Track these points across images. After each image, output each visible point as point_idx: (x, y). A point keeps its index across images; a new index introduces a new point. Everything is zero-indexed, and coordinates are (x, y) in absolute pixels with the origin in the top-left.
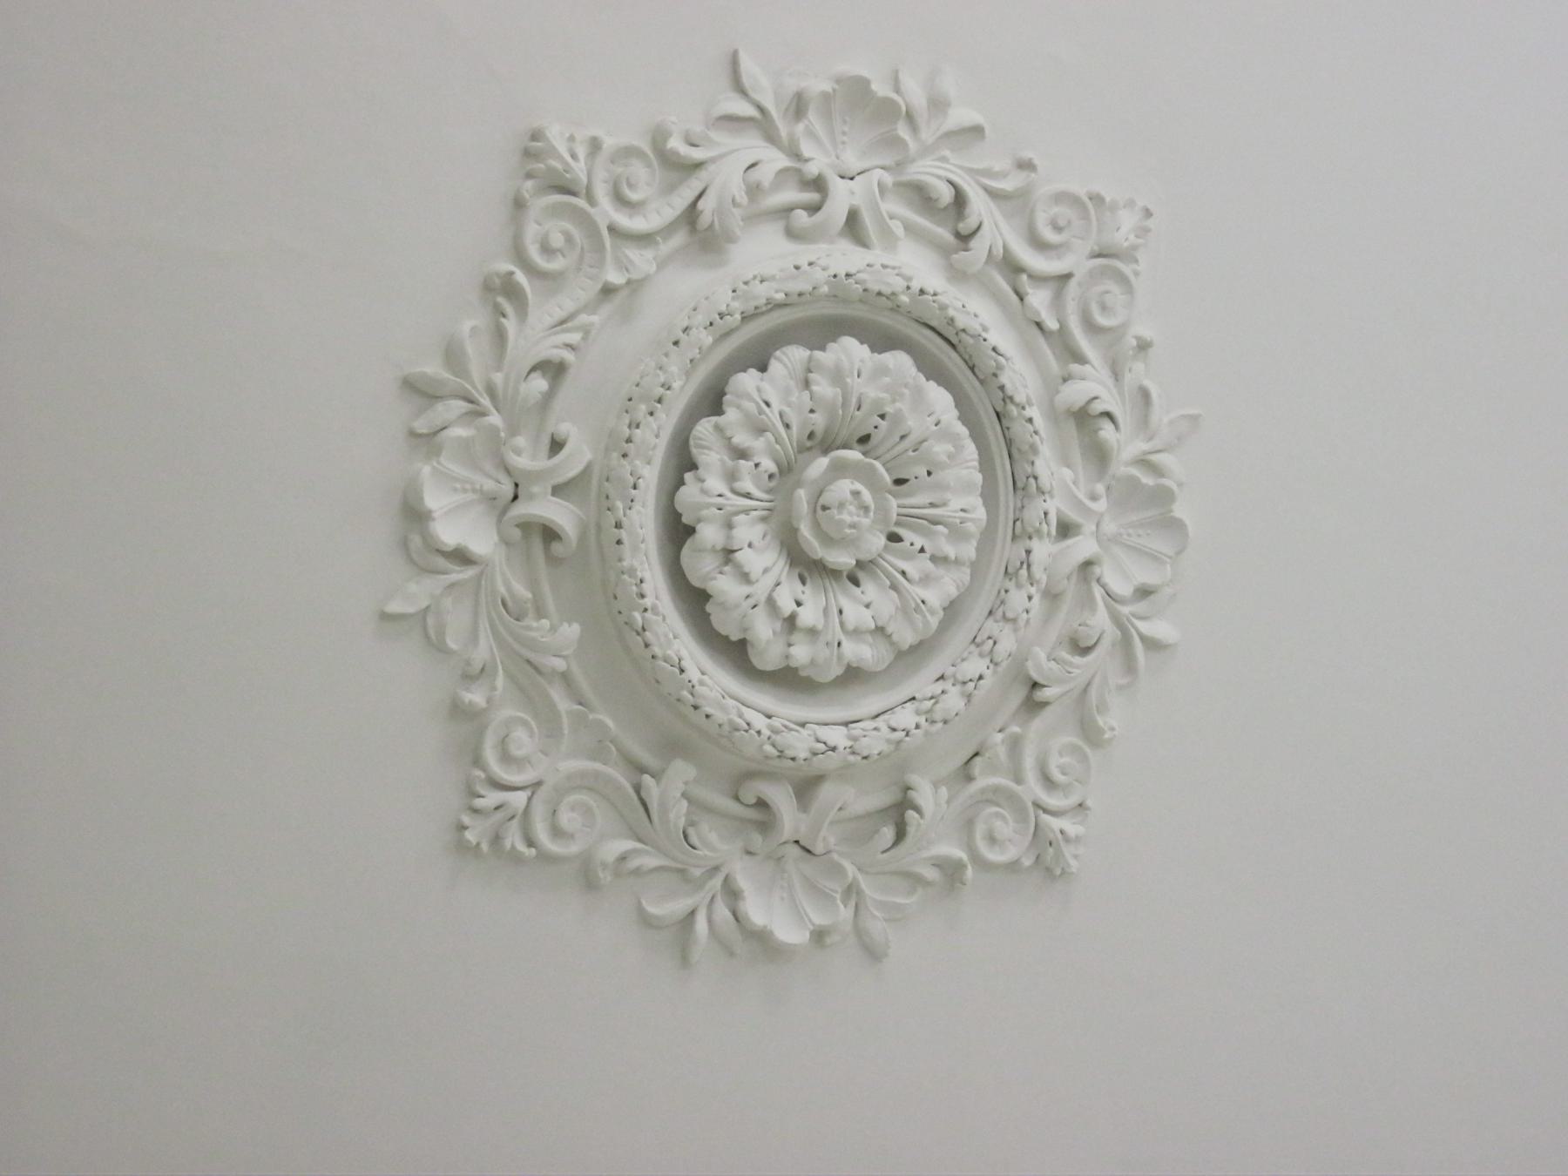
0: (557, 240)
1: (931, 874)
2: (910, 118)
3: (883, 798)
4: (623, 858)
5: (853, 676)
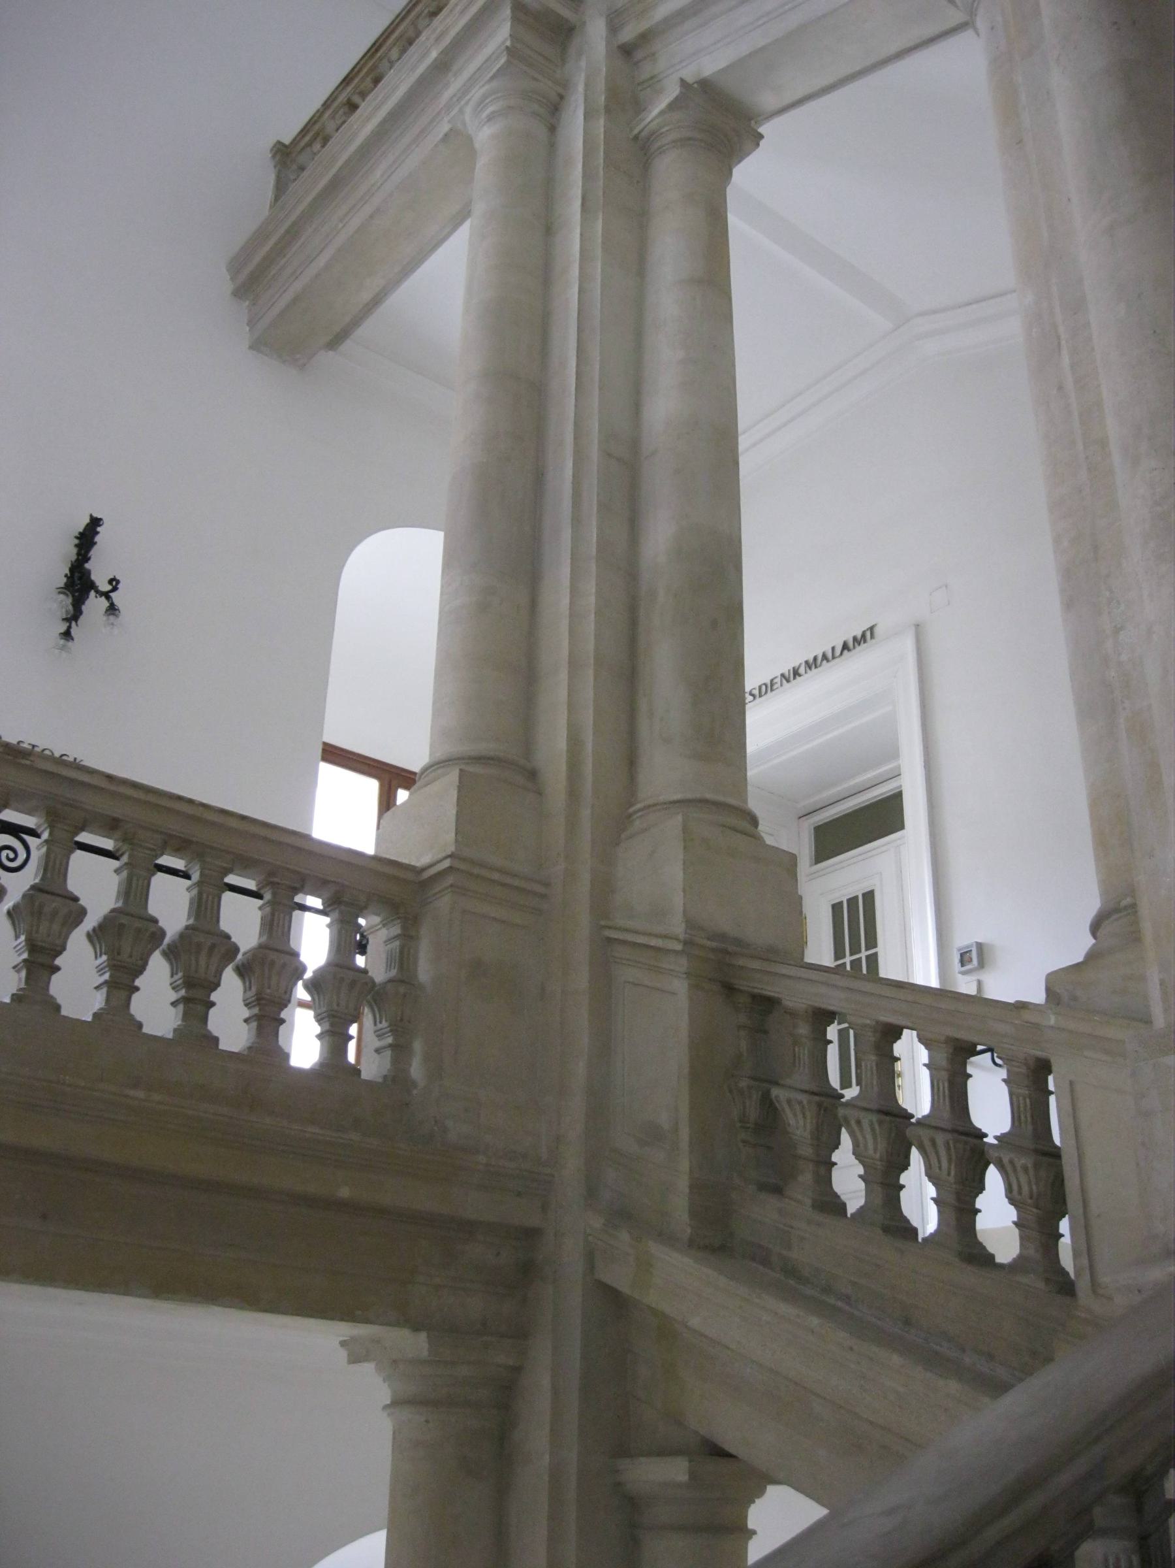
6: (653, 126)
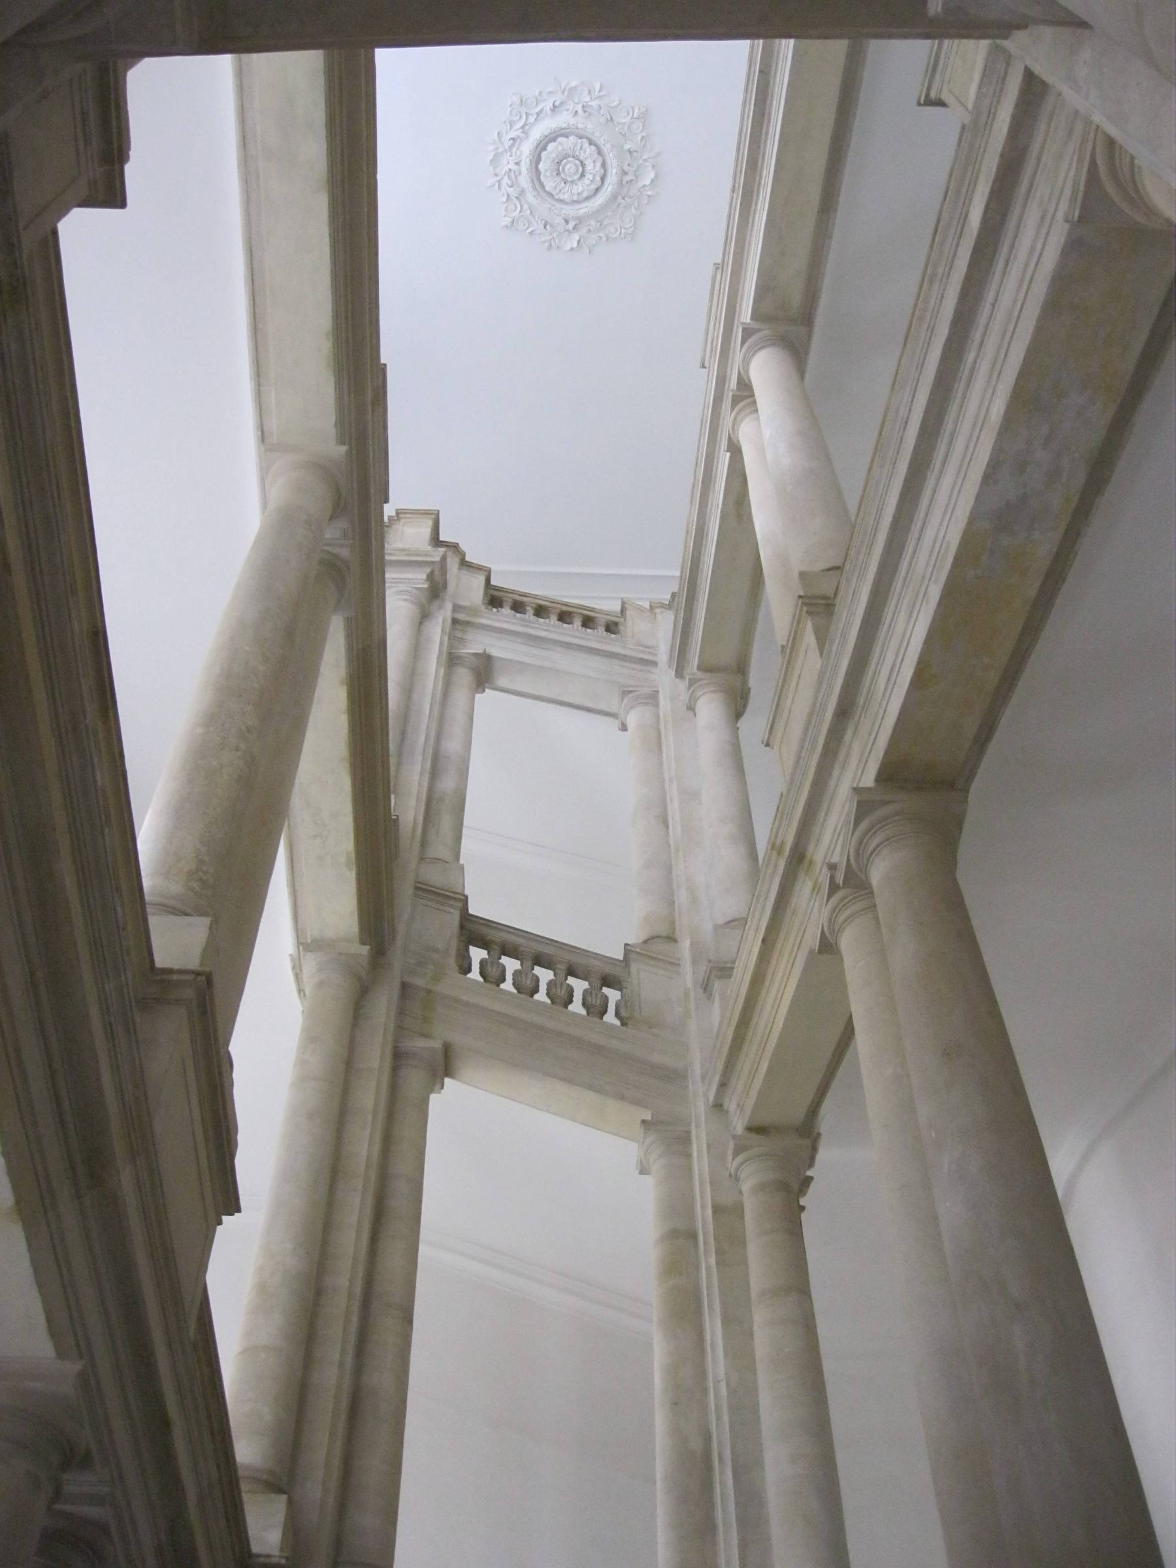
0: (522, 224)
1: (643, 143)
2: (497, 149)
3: (628, 155)
4: (636, 208)
5: (604, 165)
6: (462, 655)
